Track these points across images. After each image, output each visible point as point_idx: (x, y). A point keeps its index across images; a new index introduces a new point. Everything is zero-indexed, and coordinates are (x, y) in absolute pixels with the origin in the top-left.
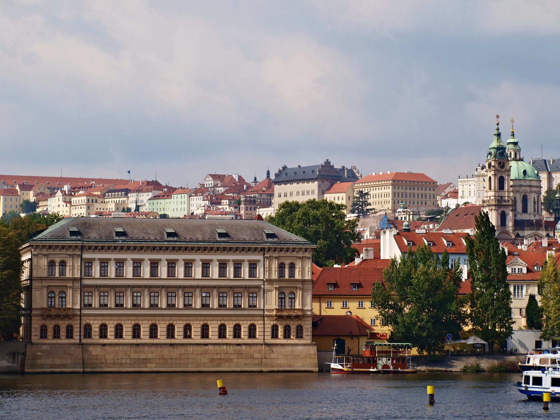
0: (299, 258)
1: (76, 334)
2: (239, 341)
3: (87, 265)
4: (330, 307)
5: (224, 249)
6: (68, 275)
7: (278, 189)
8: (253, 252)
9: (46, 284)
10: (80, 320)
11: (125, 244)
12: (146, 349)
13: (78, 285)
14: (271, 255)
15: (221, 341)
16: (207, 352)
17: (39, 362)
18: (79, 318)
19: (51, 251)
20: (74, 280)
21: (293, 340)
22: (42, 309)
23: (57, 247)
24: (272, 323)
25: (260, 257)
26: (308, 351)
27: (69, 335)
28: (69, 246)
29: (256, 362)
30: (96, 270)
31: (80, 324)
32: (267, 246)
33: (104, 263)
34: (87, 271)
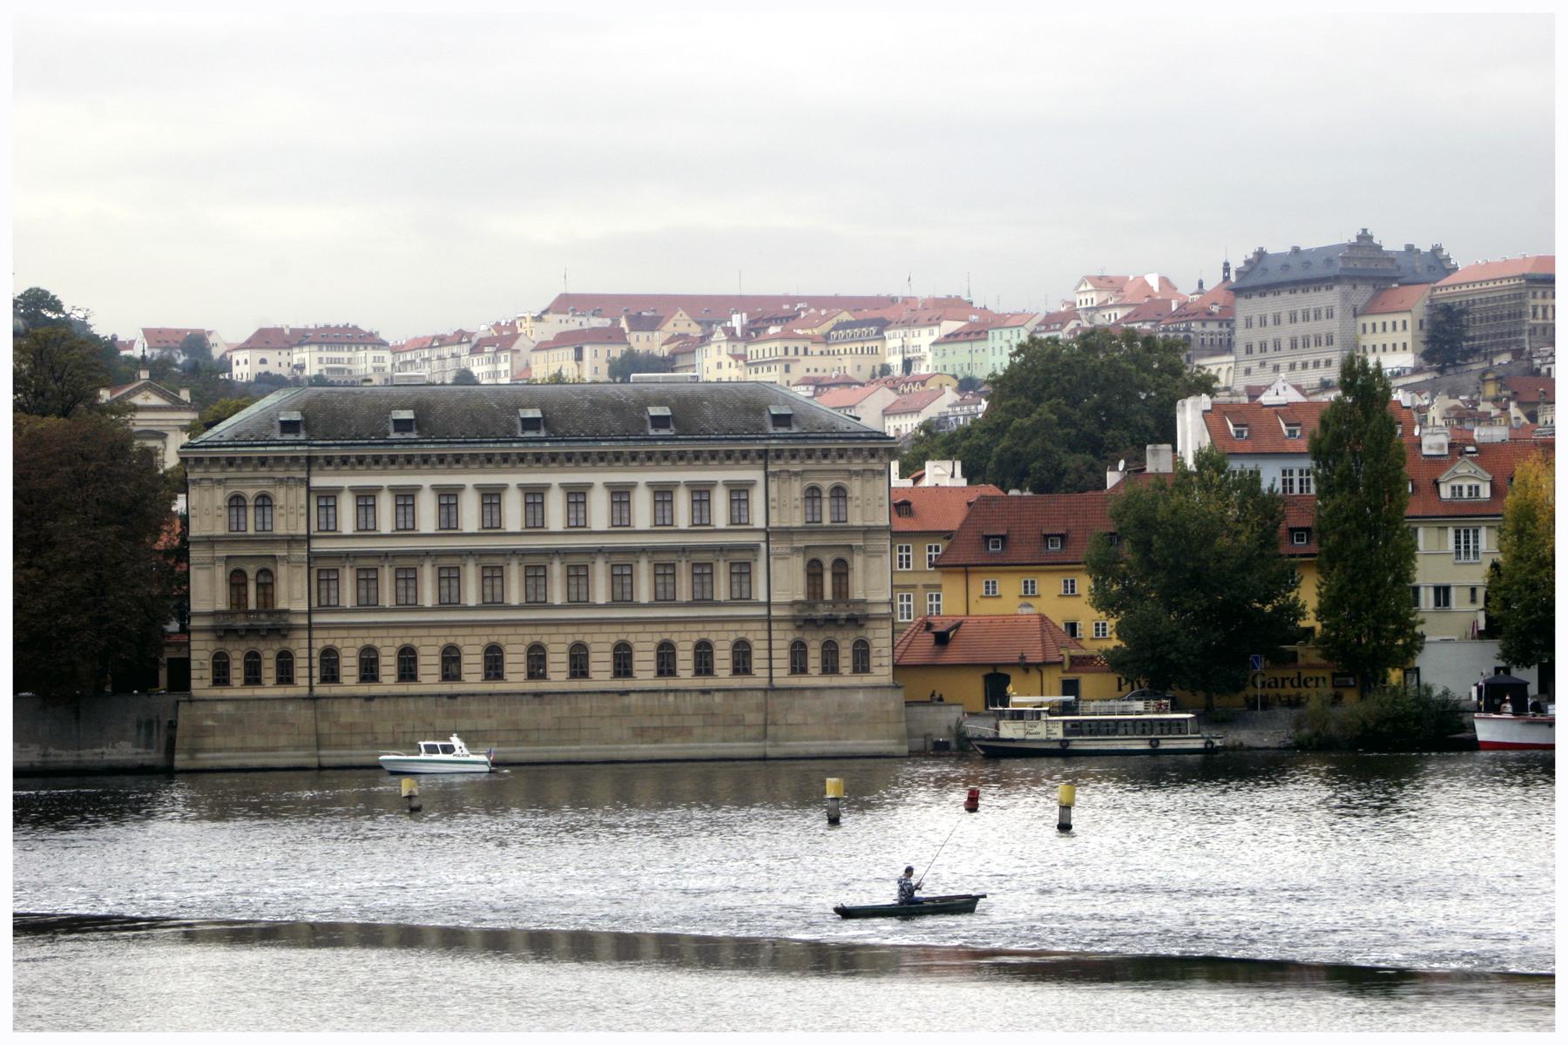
0: (857, 473)
1: (301, 672)
2: (709, 682)
3: (323, 503)
4: (991, 593)
5: (666, 456)
6: (281, 529)
7: (1245, 308)
8: (721, 463)
9: (222, 552)
10: (310, 639)
11: (415, 450)
12: (474, 706)
13: (300, 553)
14: (785, 467)
15: (662, 683)
16: (626, 710)
17: (208, 742)
18: (306, 634)
19: (231, 472)
20: (291, 540)
21: (846, 678)
22: (215, 614)
23: (247, 460)
24: (790, 637)
25: (755, 474)
26: (882, 704)
27: (285, 676)
28: (244, 459)
29: (751, 732)
30: (347, 517)
31: (310, 648)
32: (774, 444)
33: (366, 499)
34: (323, 519)
